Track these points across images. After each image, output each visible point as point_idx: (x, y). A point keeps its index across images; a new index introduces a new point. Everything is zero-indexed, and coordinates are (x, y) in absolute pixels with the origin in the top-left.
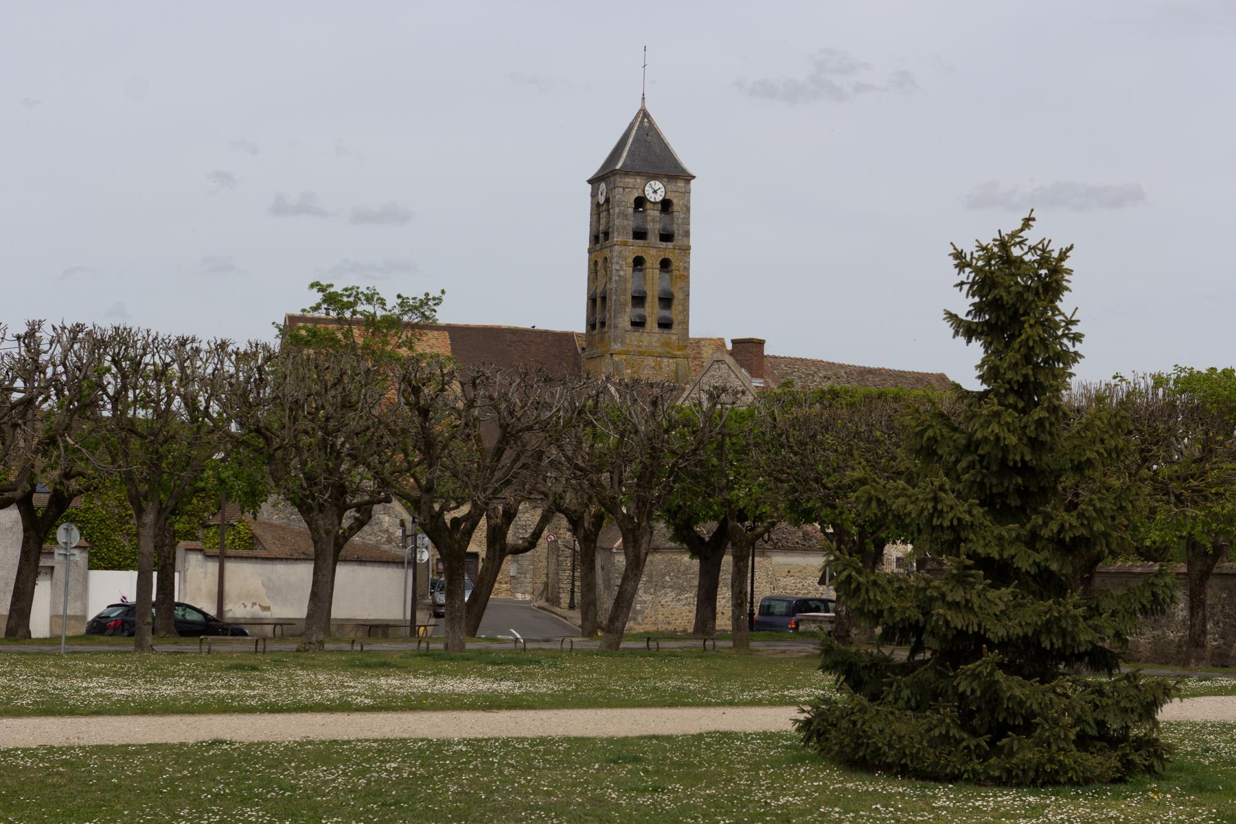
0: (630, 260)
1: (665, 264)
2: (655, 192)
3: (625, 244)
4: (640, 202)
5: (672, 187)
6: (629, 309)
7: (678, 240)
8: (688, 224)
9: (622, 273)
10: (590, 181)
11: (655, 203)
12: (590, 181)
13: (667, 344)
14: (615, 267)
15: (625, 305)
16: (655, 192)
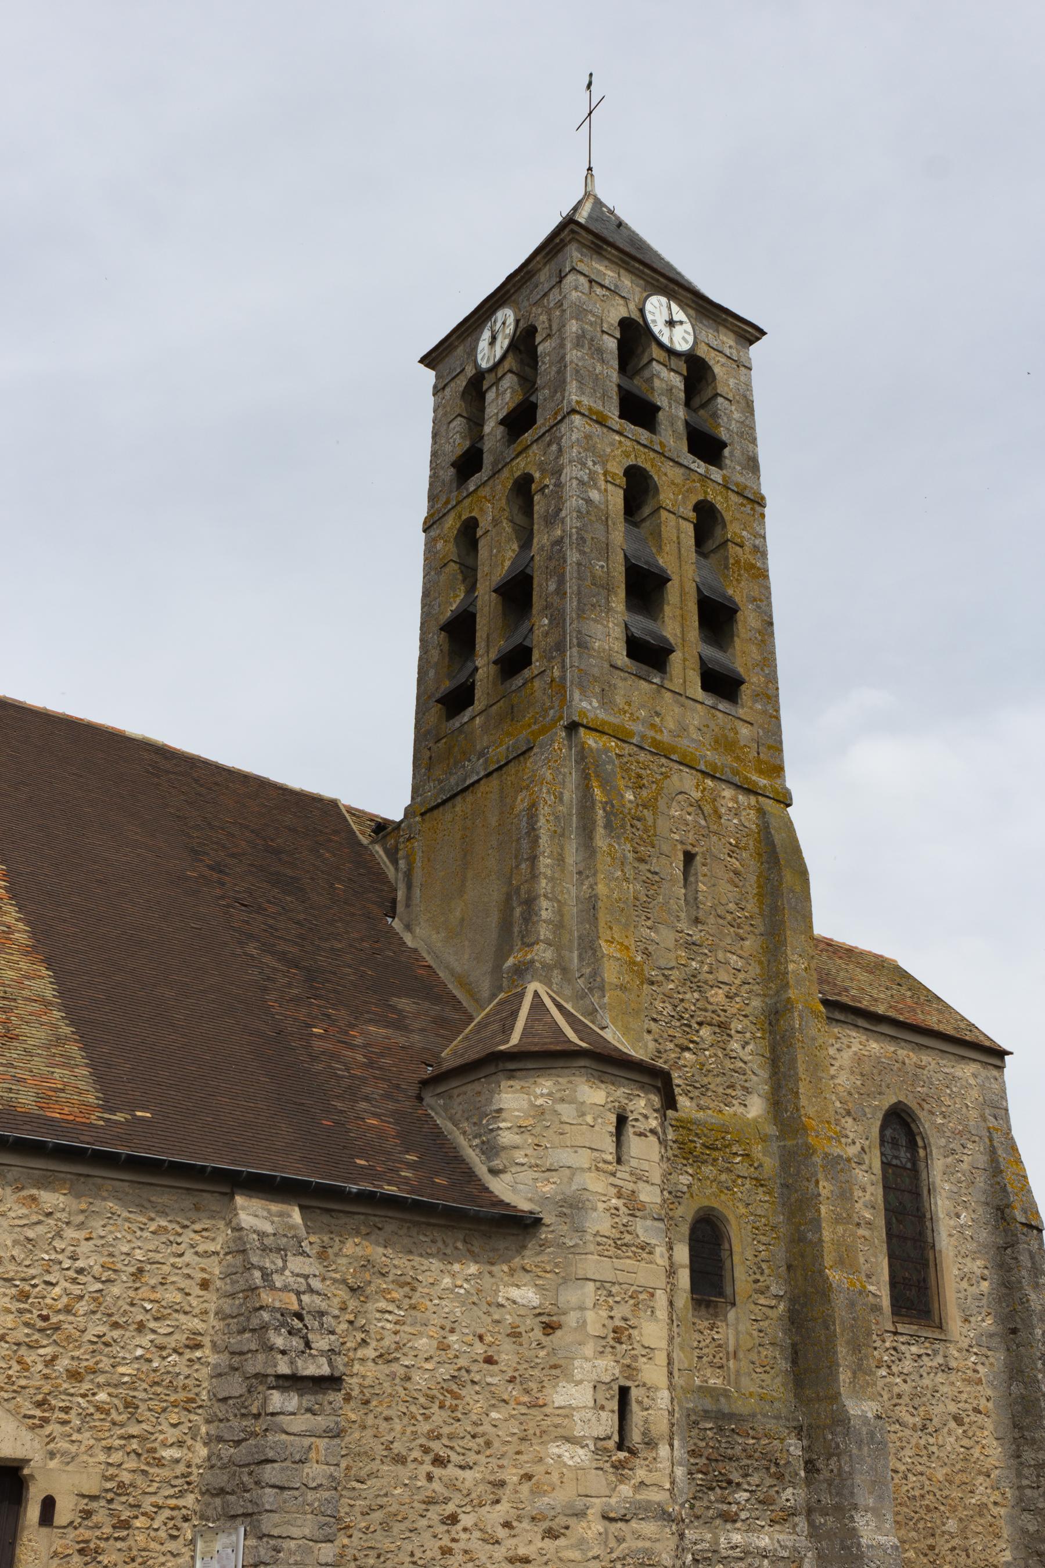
0: (617, 469)
1: (707, 520)
2: (671, 323)
3: (601, 421)
4: (634, 336)
5: (709, 335)
6: (618, 602)
7: (733, 468)
8: (754, 441)
9: (595, 495)
10: (429, 360)
11: (671, 352)
12: (429, 360)
13: (726, 744)
14: (571, 472)
15: (608, 589)
16: (671, 323)
